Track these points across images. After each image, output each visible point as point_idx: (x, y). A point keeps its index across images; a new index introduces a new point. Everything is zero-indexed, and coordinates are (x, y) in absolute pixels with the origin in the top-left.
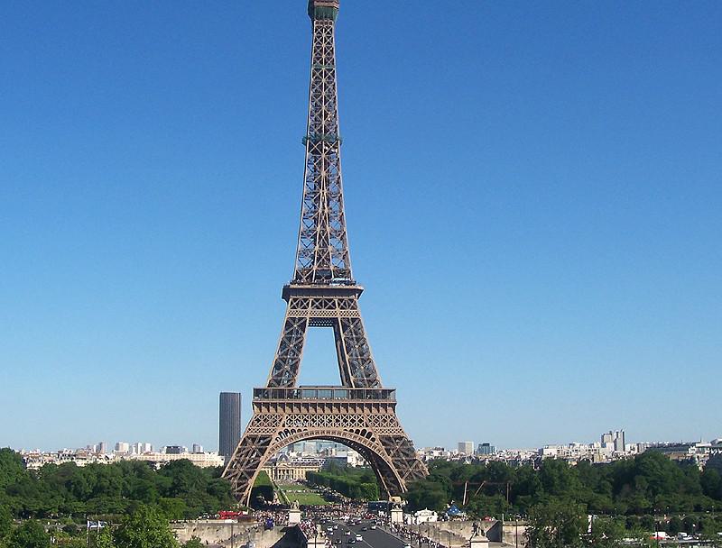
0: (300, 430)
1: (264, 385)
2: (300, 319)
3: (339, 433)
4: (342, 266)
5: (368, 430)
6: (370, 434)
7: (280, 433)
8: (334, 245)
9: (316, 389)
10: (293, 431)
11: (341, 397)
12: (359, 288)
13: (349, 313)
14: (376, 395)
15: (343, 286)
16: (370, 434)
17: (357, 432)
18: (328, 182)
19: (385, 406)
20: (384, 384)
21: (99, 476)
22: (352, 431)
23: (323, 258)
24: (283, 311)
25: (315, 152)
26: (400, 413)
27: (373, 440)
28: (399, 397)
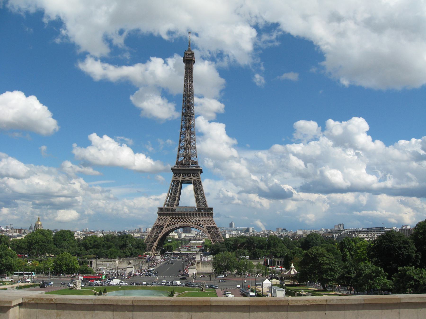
0: (175, 224)
1: (162, 206)
2: (177, 181)
3: (190, 225)
5: (202, 224)
7: (168, 225)
8: (193, 151)
9: (182, 207)
10: (173, 224)
12: (200, 168)
13: (196, 179)
14: (204, 210)
15: (194, 168)
17: (197, 224)
18: (190, 127)
19: (208, 215)
20: (209, 206)
21: (95, 241)
22: (195, 224)
23: (187, 156)
25: (185, 116)
28: (215, 212)
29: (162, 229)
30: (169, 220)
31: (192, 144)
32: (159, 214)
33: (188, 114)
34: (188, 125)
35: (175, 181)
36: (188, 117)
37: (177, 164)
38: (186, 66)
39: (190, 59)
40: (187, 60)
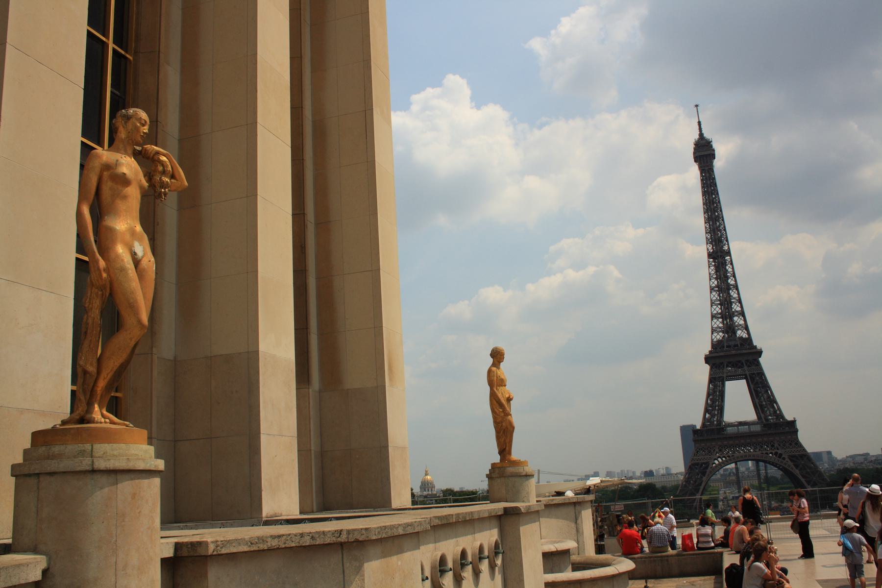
4: (745, 335)
5: (779, 452)
6: (781, 455)
11: (757, 428)
16: (781, 455)
18: (727, 278)
20: (789, 417)
24: (704, 371)
25: (714, 258)
26: (802, 437)
27: (784, 459)
28: (799, 425)
29: (707, 468)
30: (717, 450)
31: (736, 307)
32: (694, 441)
33: (719, 254)
34: (722, 273)
35: (715, 378)
36: (720, 260)
37: (713, 345)
38: (700, 168)
39: (706, 153)
40: (700, 157)
